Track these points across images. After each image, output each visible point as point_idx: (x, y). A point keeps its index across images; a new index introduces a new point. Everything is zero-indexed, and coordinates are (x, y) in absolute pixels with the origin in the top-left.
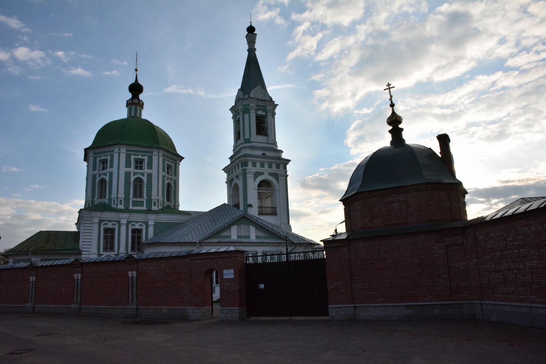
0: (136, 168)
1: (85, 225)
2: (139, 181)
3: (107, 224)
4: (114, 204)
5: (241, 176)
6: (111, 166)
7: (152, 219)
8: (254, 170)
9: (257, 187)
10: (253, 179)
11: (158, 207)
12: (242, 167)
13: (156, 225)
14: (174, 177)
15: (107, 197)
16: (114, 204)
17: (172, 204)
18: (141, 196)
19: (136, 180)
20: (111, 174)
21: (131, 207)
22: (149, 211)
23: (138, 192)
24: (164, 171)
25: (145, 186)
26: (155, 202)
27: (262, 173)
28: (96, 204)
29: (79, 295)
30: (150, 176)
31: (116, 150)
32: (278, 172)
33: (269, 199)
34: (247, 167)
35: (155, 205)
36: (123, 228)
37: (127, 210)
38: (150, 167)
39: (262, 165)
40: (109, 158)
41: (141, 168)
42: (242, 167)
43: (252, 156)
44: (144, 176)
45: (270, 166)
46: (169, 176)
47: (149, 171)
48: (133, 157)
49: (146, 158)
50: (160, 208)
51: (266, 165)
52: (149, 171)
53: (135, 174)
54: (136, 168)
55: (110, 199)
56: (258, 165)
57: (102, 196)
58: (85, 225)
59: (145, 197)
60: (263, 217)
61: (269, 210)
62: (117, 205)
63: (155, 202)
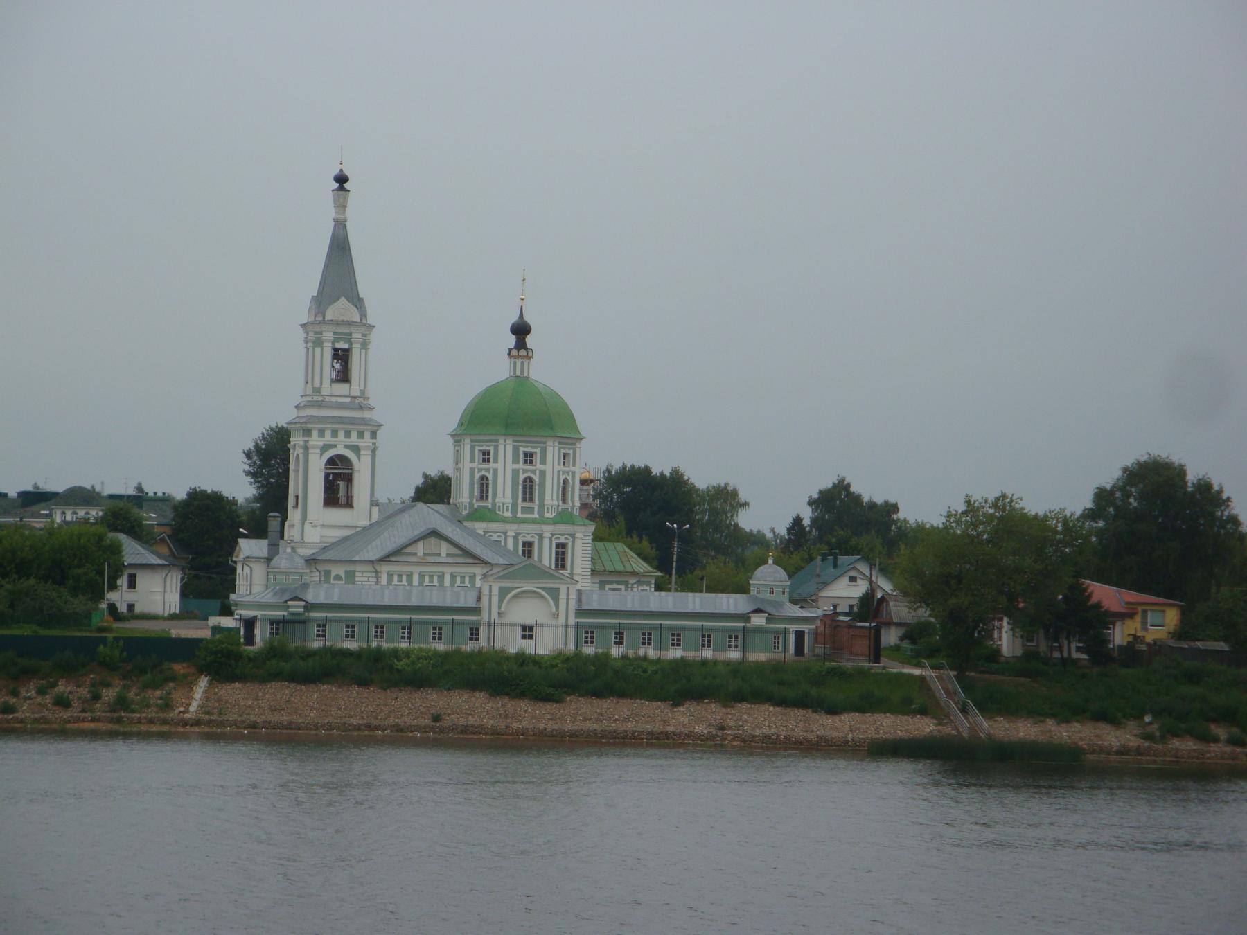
0: (525, 462)
2: (529, 481)
6: (496, 461)
18: (531, 500)
19: (525, 480)
20: (495, 471)
21: (519, 515)
22: (542, 521)
23: (528, 495)
30: (543, 474)
37: (515, 520)
38: (543, 462)
47: (543, 467)
49: (538, 450)
52: (543, 467)
53: (525, 471)
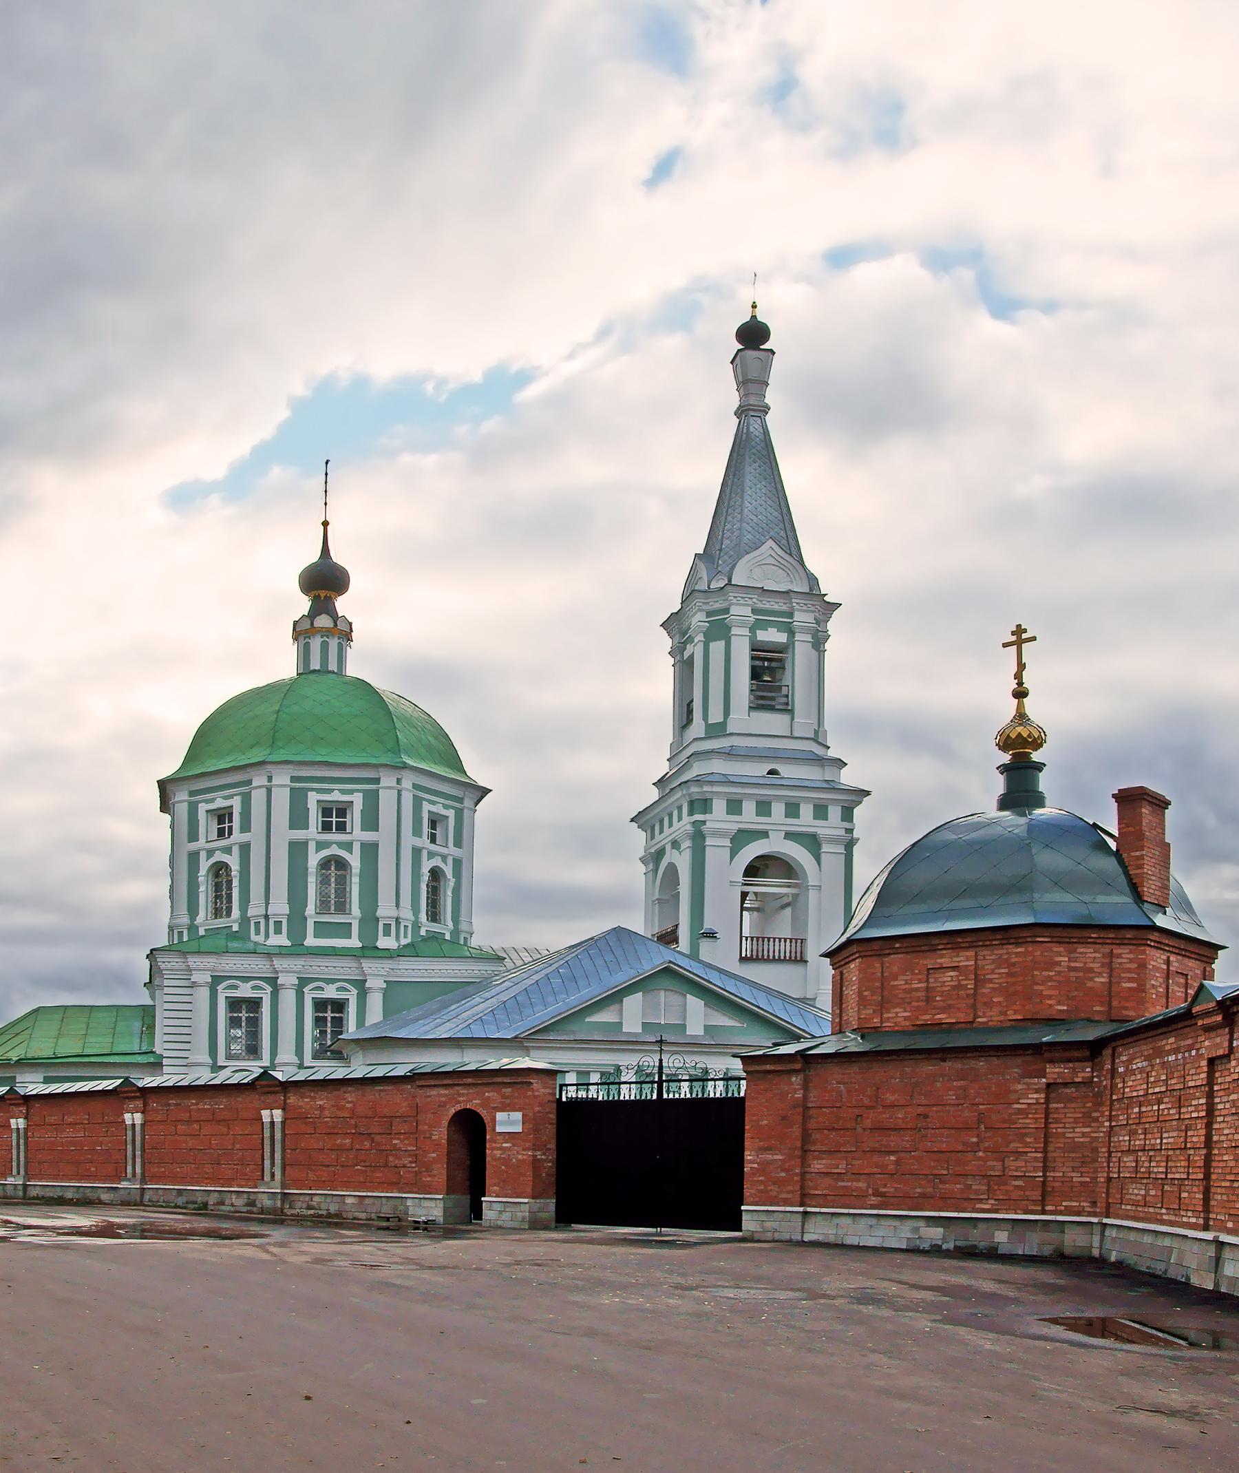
0: (326, 827)
1: (166, 990)
3: (236, 987)
4: (258, 932)
5: (686, 844)
6: (246, 827)
7: (377, 974)
8: (733, 824)
9: (739, 877)
10: (728, 851)
11: (398, 938)
12: (691, 813)
13: (391, 987)
14: (457, 852)
15: (236, 913)
16: (258, 932)
17: (445, 928)
18: (342, 907)
19: (325, 864)
20: (245, 849)
22: (370, 951)
24: (417, 832)
25: (356, 880)
26: (387, 927)
27: (764, 834)
28: (202, 932)
29: (138, 1160)
31: (259, 780)
32: (820, 831)
33: (788, 910)
34: (707, 817)
35: (387, 933)
36: (288, 999)
37: (297, 949)
39: (764, 808)
40: (236, 803)
41: (341, 827)
42: (691, 813)
43: (727, 781)
44: (350, 850)
45: (792, 810)
46: (433, 847)
47: (369, 836)
48: (313, 799)
50: (404, 942)
51: (778, 809)
52: (369, 836)
53: (321, 846)
54: (326, 827)
55: (245, 920)
56: (749, 807)
57: (221, 906)
58: (166, 990)
59: (356, 910)
60: (756, 973)
61: (785, 949)
62: (267, 936)
63: (387, 927)
